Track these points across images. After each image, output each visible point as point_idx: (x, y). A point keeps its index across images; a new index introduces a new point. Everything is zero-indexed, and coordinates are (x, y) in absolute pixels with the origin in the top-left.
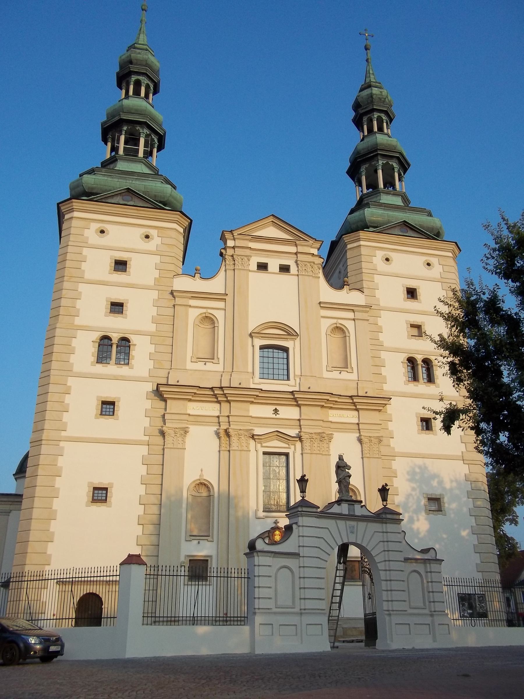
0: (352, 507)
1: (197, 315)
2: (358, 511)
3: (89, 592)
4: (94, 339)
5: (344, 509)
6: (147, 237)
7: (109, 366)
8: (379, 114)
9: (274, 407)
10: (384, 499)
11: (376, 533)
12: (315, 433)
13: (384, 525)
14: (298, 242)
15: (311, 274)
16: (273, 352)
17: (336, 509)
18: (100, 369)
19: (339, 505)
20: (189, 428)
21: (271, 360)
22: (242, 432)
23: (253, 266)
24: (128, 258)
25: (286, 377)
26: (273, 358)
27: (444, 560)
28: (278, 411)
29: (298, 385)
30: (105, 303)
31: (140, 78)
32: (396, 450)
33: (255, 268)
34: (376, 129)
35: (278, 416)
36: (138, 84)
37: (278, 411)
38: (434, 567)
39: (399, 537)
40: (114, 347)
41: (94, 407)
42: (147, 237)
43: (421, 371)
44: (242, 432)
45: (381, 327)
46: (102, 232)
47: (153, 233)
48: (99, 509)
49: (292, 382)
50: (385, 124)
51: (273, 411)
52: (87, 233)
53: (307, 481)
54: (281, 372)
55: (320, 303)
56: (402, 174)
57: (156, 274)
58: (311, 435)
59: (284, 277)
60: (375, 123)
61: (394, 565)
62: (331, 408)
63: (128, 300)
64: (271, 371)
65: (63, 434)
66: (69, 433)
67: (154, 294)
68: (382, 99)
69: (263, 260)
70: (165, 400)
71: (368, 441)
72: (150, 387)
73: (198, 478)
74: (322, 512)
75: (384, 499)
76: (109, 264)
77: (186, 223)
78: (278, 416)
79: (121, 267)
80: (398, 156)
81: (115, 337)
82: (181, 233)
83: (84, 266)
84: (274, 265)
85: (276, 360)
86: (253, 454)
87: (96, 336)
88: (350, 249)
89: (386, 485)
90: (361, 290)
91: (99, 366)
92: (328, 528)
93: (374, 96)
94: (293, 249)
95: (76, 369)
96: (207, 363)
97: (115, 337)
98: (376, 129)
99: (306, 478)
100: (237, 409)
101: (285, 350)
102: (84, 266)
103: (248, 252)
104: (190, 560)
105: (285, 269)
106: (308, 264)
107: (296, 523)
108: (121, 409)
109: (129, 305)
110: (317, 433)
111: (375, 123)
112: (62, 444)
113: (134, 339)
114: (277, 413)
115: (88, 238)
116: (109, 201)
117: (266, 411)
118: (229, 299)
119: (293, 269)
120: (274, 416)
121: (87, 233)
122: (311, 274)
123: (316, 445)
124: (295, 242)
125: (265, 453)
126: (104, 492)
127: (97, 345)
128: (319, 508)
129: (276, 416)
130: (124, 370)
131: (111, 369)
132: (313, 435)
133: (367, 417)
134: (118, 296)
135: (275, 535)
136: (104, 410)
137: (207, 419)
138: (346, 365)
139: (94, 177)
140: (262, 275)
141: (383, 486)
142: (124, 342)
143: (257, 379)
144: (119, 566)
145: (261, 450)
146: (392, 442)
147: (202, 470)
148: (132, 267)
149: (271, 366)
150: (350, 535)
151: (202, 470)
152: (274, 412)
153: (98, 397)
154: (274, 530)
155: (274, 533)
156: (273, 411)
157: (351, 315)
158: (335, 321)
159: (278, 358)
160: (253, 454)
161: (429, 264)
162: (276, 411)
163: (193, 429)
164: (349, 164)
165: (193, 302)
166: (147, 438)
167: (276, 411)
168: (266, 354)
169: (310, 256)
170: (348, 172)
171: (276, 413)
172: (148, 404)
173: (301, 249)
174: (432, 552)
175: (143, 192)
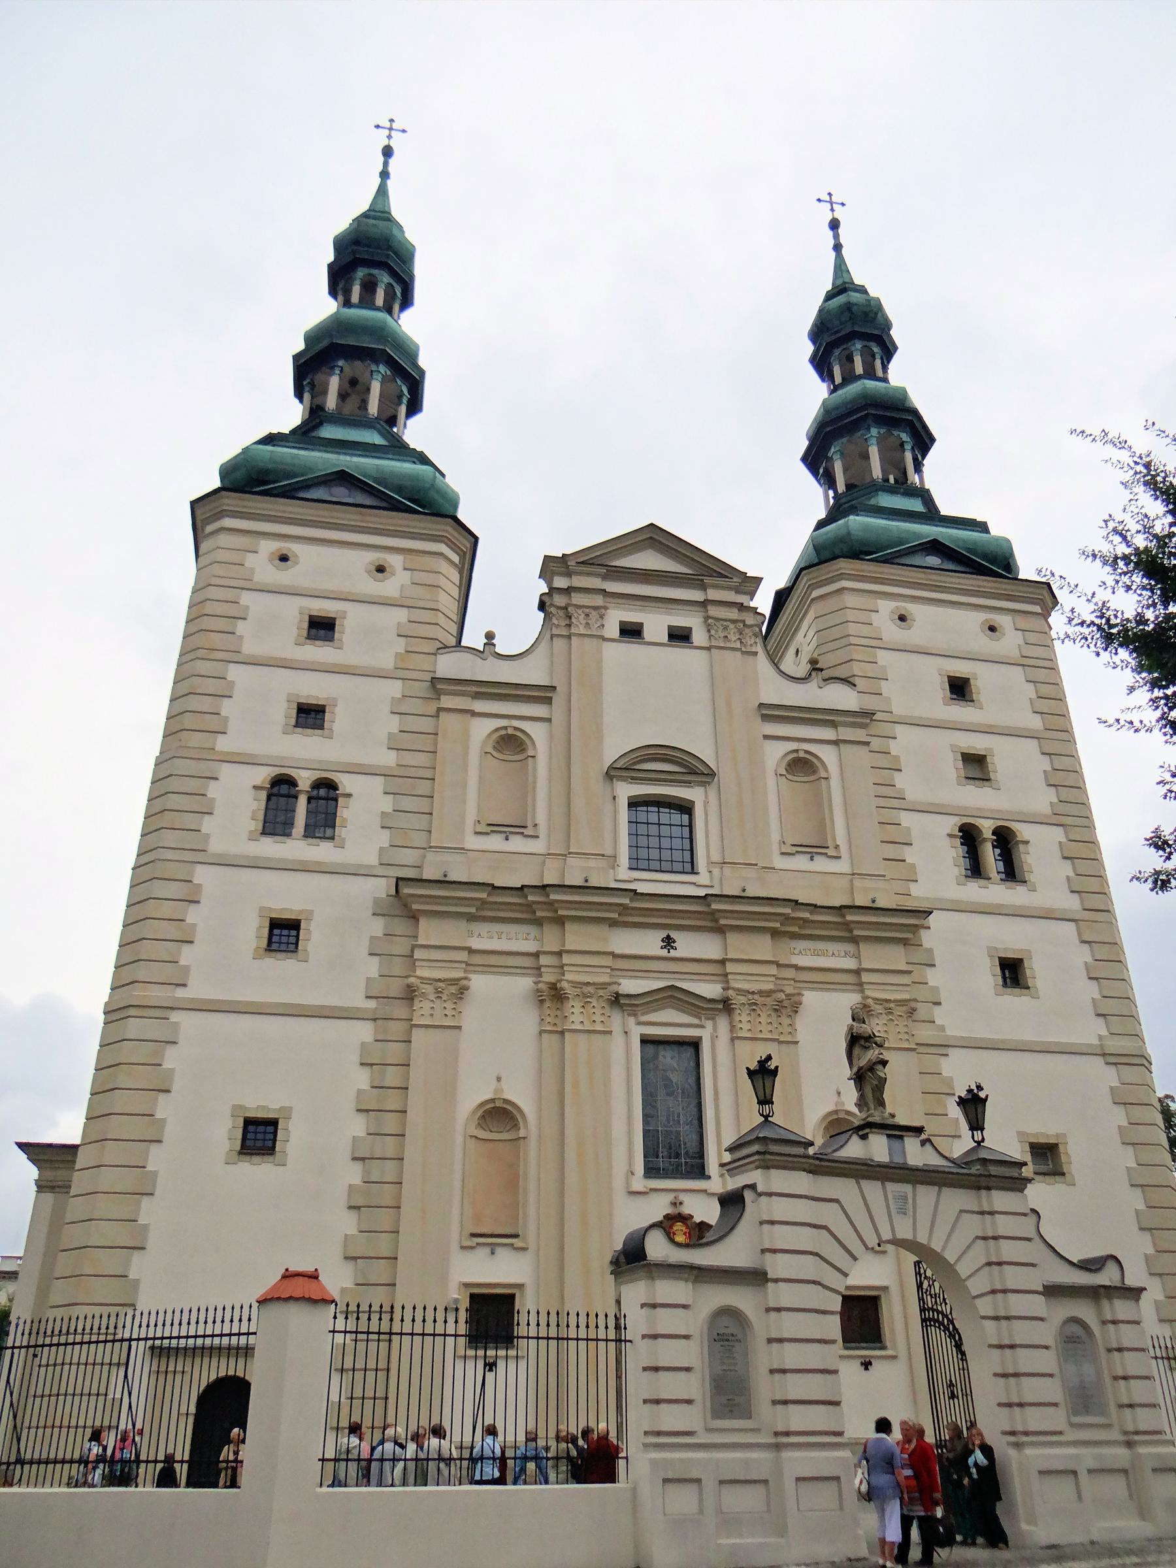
0: (896, 1144)
1: (489, 732)
2: (915, 1154)
3: (233, 1374)
4: (258, 783)
5: (878, 1148)
6: (380, 569)
7: (289, 842)
8: (865, 343)
9: (664, 934)
10: (976, 1125)
11: (964, 1215)
13: (984, 1193)
14: (707, 580)
15: (738, 645)
16: (659, 812)
17: (854, 1149)
18: (271, 848)
19: (864, 1137)
20: (470, 980)
21: (654, 830)
22: (591, 989)
23: (613, 631)
24: (337, 612)
25: (688, 867)
26: (659, 824)
27: (1145, 1289)
28: (674, 942)
29: (716, 883)
30: (285, 705)
31: (375, 272)
32: (949, 1032)
33: (615, 633)
34: (859, 369)
35: (673, 953)
36: (369, 287)
37: (674, 942)
38: (1122, 1308)
39: (1025, 1227)
40: (302, 802)
41: (253, 932)
42: (380, 569)
43: (990, 855)
44: (591, 989)
45: (897, 759)
46: (284, 558)
48: (258, 1171)
49: (703, 878)
50: (878, 363)
51: (663, 941)
52: (250, 560)
53: (775, 1072)
54: (677, 856)
55: (761, 705)
56: (920, 459)
57: (400, 645)
58: (750, 997)
59: (679, 653)
60: (858, 360)
61: (1018, 1305)
62: (794, 936)
63: (335, 699)
64: (654, 854)
65: (180, 993)
66: (195, 990)
67: (394, 688)
68: (872, 315)
69: (632, 617)
70: (414, 917)
72: (381, 888)
73: (489, 1096)
74: (815, 1157)
75: (976, 1125)
78: (673, 953)
79: (322, 632)
80: (910, 418)
81: (305, 781)
82: (455, 565)
84: (656, 625)
85: (665, 831)
86: (618, 1040)
87: (263, 775)
89: (980, 1088)
90: (848, 681)
91: (267, 841)
92: (836, 1201)
93: (854, 309)
94: (696, 595)
95: (217, 846)
96: (511, 837)
97: (305, 781)
98: (859, 369)
99: (772, 1065)
100: (577, 937)
101: (686, 808)
102: (241, 628)
103: (598, 600)
104: (472, 1296)
105: (679, 636)
106: (732, 626)
107: (753, 1187)
108: (313, 938)
109: (338, 710)
110: (765, 992)
111: (858, 360)
112: (175, 1017)
113: (346, 783)
114: (672, 947)
116: (302, 495)
117: (648, 943)
118: (558, 700)
120: (664, 953)
121: (250, 560)
122: (738, 645)
124: (702, 580)
125: (645, 1041)
126: (270, 1129)
127: (263, 795)
128: (812, 1144)
129: (669, 952)
130: (321, 851)
131: (295, 848)
132: (756, 997)
133: (875, 956)
134: (312, 689)
135: (674, 1234)
136: (275, 939)
137: (511, 961)
138: (817, 848)
139: (269, 448)
140: (631, 649)
141: (970, 1091)
142: (322, 792)
143: (623, 872)
144: (255, 1305)
145: (637, 1032)
146: (939, 1015)
147: (499, 1079)
148: (347, 630)
149: (654, 842)
150: (897, 1219)
151: (499, 1079)
153: (261, 909)
155: (671, 1227)
157: (828, 734)
158: (794, 746)
159: (670, 825)
160: (618, 1040)
161: (992, 629)
162: (669, 942)
163: (479, 983)
164: (806, 443)
165: (480, 706)
166: (372, 1004)
167: (669, 942)
168: (642, 817)
170: (804, 459)
171: (669, 944)
172: (377, 927)
173: (713, 594)
174: (1111, 1267)
175: (375, 480)
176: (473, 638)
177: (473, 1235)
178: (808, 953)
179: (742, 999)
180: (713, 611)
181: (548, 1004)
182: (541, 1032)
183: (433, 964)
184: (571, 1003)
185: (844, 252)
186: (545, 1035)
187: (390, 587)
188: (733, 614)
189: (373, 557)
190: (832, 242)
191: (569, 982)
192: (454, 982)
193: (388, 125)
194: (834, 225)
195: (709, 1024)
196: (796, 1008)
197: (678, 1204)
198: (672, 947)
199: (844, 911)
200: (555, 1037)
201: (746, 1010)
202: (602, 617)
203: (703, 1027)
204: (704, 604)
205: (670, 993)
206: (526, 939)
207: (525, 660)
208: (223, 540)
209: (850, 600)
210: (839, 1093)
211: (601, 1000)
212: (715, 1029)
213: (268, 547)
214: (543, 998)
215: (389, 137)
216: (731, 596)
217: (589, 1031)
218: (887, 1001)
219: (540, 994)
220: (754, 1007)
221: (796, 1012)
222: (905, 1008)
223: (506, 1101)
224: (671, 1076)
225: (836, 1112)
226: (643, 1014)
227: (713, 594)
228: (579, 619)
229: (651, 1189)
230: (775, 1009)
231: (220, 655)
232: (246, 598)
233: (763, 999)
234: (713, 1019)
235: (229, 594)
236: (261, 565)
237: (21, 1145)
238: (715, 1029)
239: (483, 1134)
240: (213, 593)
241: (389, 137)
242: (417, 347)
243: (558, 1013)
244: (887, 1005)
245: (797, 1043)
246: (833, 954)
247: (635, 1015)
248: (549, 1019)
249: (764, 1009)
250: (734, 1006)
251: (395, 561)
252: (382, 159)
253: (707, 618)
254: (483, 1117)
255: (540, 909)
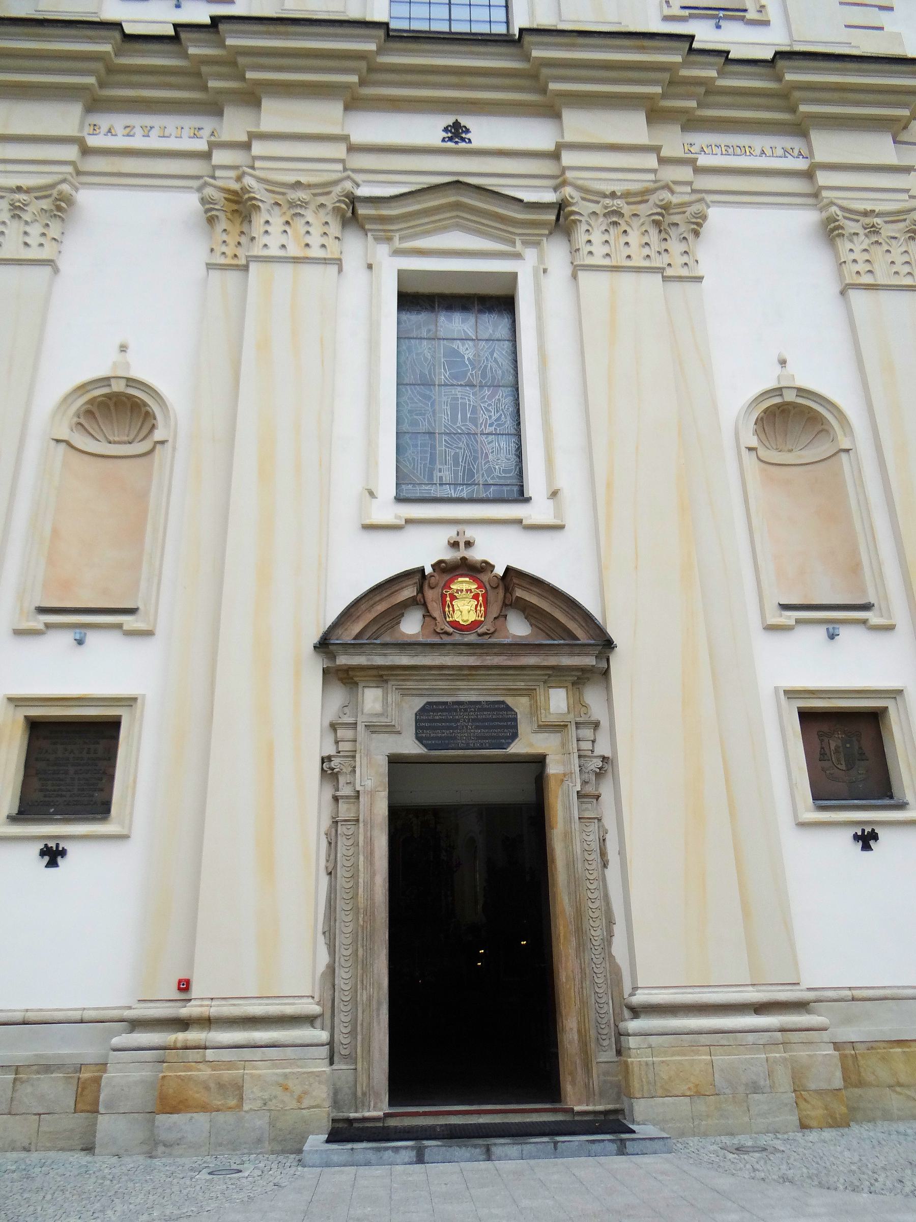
9: (449, 120)
12: (626, 195)
28: (467, 131)
51: (446, 130)
58: (608, 201)
71: (861, 232)
110: (636, 194)
123: (634, 237)
135: (453, 598)
147: (123, 348)
151: (123, 348)
152: (450, 135)
154: (446, 577)
155: (447, 586)
156: (446, 130)
162: (456, 132)
167: (456, 132)
177: (43, 610)
178: (715, 150)
179: (593, 207)
181: (223, 224)
182: (210, 266)
183: (10, 167)
184: (264, 216)
186: (215, 275)
191: (260, 180)
192: (41, 192)
195: (530, 254)
196: (697, 226)
197: (462, 545)
198: (463, 140)
199: (781, 63)
200: (232, 277)
201: (600, 225)
203: (518, 256)
205: (452, 199)
206: (195, 136)
210: (783, 363)
211: (322, 212)
212: (541, 258)
214: (214, 213)
217: (296, 260)
218: (866, 214)
219: (208, 206)
220: (615, 219)
221: (697, 234)
222: (901, 225)
223: (131, 382)
224: (462, 350)
225: (779, 391)
226: (401, 239)
229: (409, 521)
230: (654, 221)
233: (633, 207)
234: (537, 244)
238: (541, 258)
239: (82, 441)
243: (243, 240)
244: (867, 220)
245: (699, 279)
246: (763, 152)
247: (389, 239)
248: (224, 249)
249: (635, 223)
250: (577, 217)
254: (89, 413)
255: (197, 43)
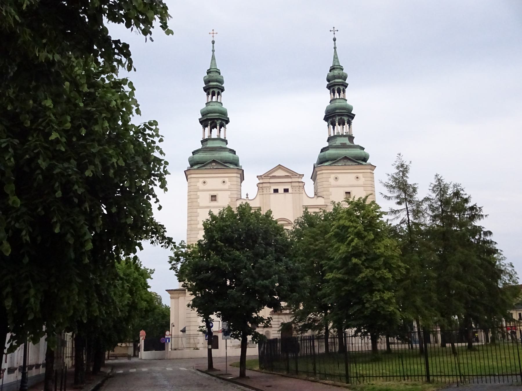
8: (339, 87)
31: (214, 90)
42: (224, 182)
46: (204, 182)
47: (226, 180)
59: (287, 194)
69: (276, 188)
76: (209, 198)
77: (241, 172)
83: (199, 200)
84: (281, 190)
88: (319, 174)
94: (290, 180)
102: (199, 200)
103: (268, 185)
105: (286, 191)
115: (199, 186)
119: (290, 191)
140: (276, 195)
148: (219, 198)
161: (357, 178)
169: (298, 183)
176: (244, 196)
180: (293, 184)
185: (337, 49)
187: (226, 186)
188: (297, 184)
189: (222, 180)
190: (333, 46)
193: (212, 32)
194: (335, 40)
202: (270, 189)
204: (291, 182)
207: (254, 200)
208: (193, 180)
209: (324, 176)
213: (201, 180)
215: (213, 36)
216: (297, 180)
227: (294, 180)
228: (265, 190)
231: (195, 207)
232: (199, 193)
235: (195, 193)
236: (200, 185)
237: (166, 290)
240: (192, 193)
241: (213, 36)
242: (226, 109)
251: (226, 180)
252: (212, 44)
253: (292, 186)
